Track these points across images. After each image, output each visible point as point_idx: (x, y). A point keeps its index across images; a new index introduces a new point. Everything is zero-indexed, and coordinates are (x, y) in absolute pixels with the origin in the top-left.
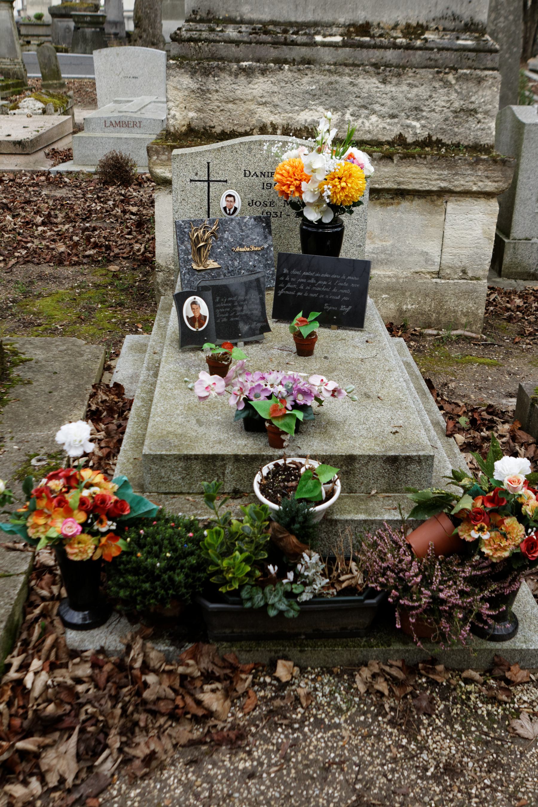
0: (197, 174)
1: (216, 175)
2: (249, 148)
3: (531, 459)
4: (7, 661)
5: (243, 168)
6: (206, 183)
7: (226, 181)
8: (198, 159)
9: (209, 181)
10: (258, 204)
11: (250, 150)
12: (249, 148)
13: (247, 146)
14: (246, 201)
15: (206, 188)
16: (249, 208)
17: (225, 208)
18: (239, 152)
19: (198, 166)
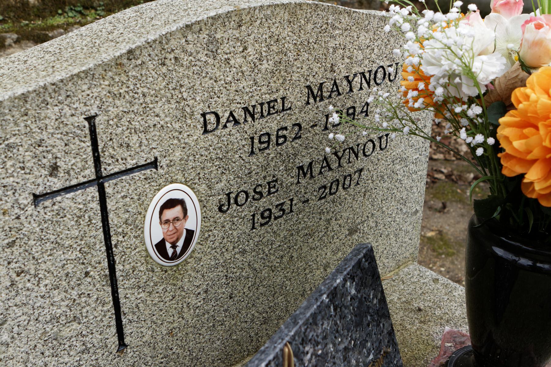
0: (54, 169)
1: (121, 153)
2: (212, 40)
3: (483, 155)
4: (329, 258)
5: (199, 109)
6: (93, 191)
7: (154, 164)
8: (52, 112)
9: (99, 181)
10: (242, 198)
11: (213, 47)
12: (212, 40)
13: (204, 35)
14: (214, 202)
15: (96, 206)
16: (221, 218)
17: (161, 247)
18: (185, 59)
19: (56, 142)
